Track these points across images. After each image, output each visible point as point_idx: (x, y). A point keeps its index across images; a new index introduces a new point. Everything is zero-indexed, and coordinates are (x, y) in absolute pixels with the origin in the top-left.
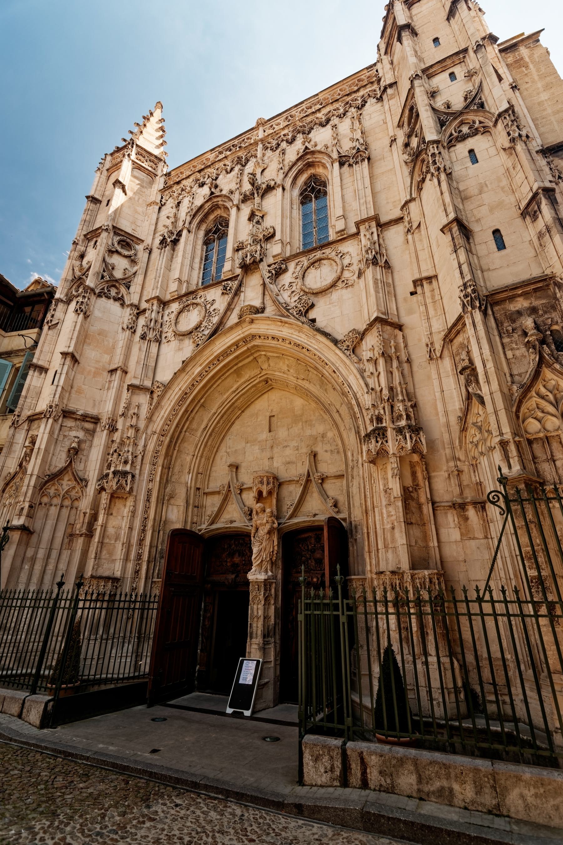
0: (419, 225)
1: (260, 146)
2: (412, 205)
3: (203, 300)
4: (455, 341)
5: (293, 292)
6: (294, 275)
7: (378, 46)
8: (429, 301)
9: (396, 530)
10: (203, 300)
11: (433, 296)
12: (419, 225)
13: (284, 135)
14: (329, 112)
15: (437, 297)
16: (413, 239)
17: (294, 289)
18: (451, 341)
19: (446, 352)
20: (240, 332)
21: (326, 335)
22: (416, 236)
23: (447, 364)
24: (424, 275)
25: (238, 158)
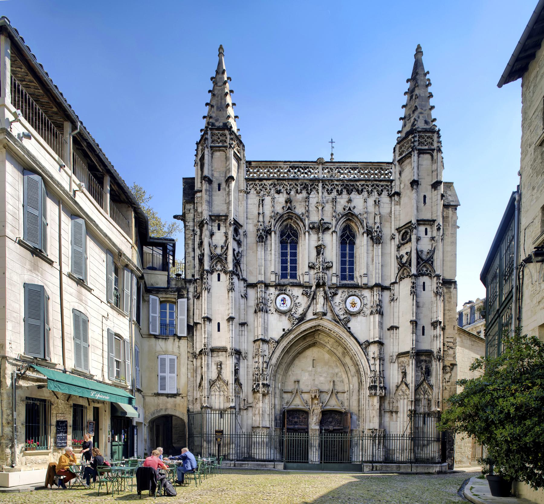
0: (397, 299)
1: (320, 185)
2: (396, 285)
3: (291, 293)
4: (400, 358)
5: (340, 309)
6: (341, 299)
7: (394, 149)
8: (394, 338)
9: (375, 418)
10: (291, 293)
11: (396, 336)
12: (397, 299)
13: (336, 185)
14: (364, 185)
15: (397, 338)
16: (394, 304)
17: (341, 307)
18: (399, 357)
19: (396, 361)
20: (314, 322)
21: (356, 339)
22: (395, 303)
23: (396, 365)
24: (395, 325)
25: (305, 184)
